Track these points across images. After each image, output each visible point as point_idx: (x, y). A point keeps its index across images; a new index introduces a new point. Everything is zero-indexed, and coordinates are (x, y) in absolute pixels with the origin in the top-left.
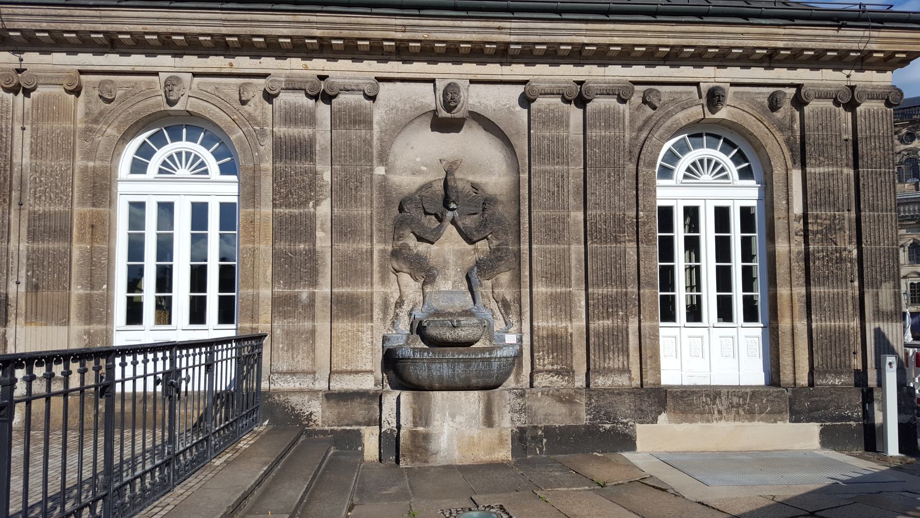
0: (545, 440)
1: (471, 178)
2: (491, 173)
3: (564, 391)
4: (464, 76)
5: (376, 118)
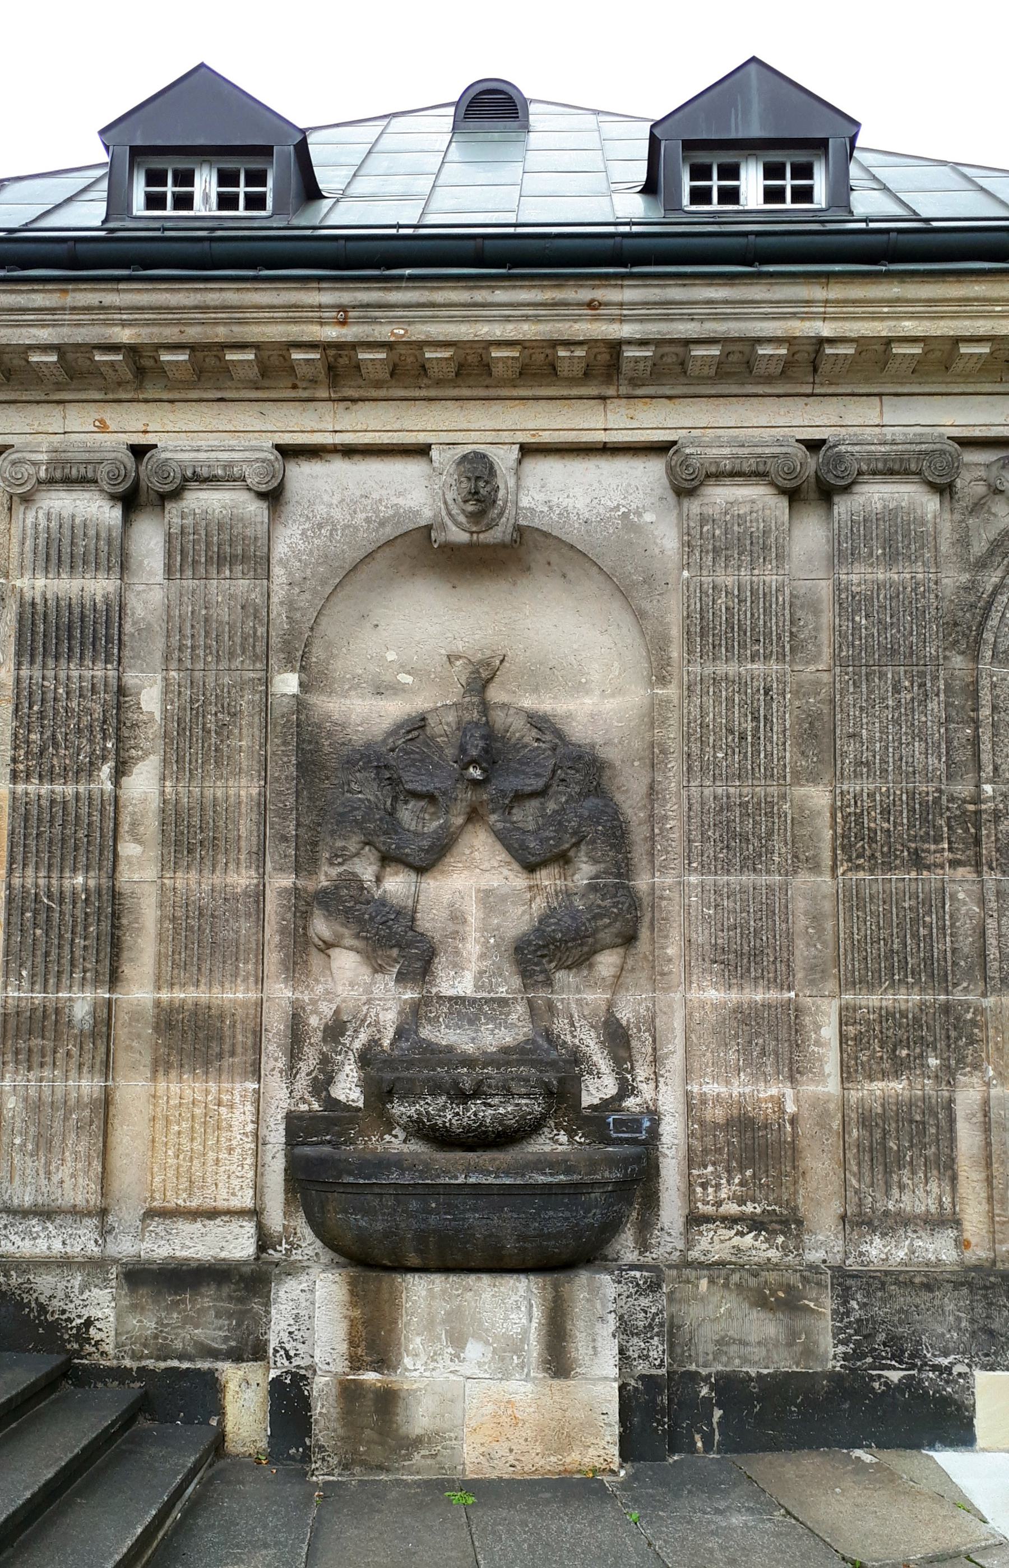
0: (718, 1413)
1: (528, 702)
2: (580, 688)
3: (772, 1277)
4: (506, 437)
5: (281, 549)
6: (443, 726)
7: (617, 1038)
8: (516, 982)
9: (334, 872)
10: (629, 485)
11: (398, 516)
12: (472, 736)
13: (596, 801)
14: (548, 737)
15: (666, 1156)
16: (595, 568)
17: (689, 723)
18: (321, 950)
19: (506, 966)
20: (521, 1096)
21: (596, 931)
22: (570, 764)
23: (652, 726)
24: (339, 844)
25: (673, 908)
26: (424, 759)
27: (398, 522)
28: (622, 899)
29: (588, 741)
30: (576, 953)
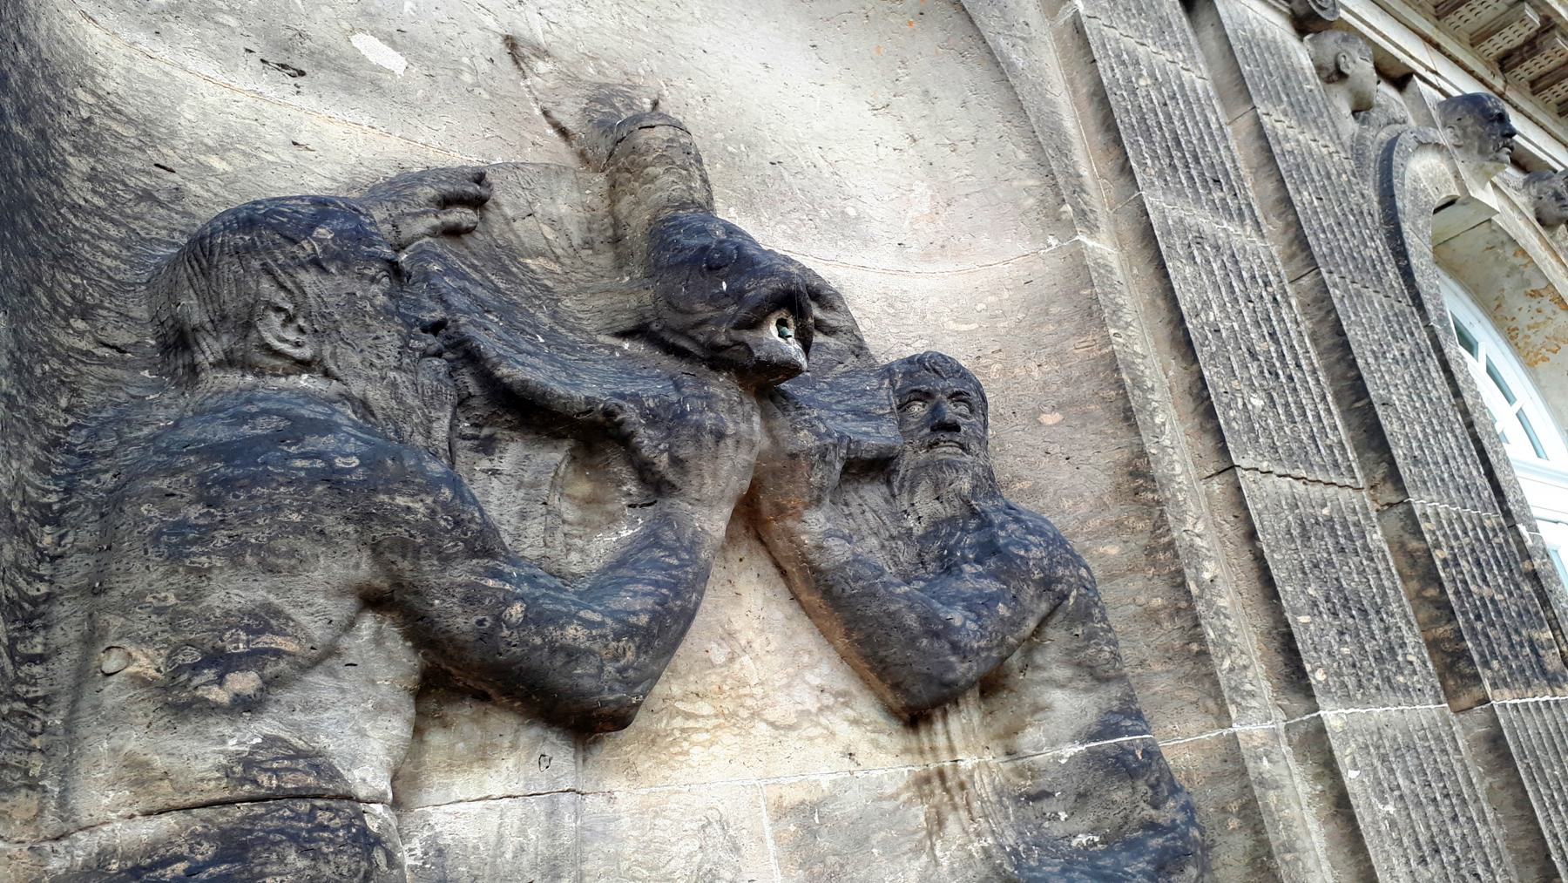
9: (202, 755)
24: (233, 593)
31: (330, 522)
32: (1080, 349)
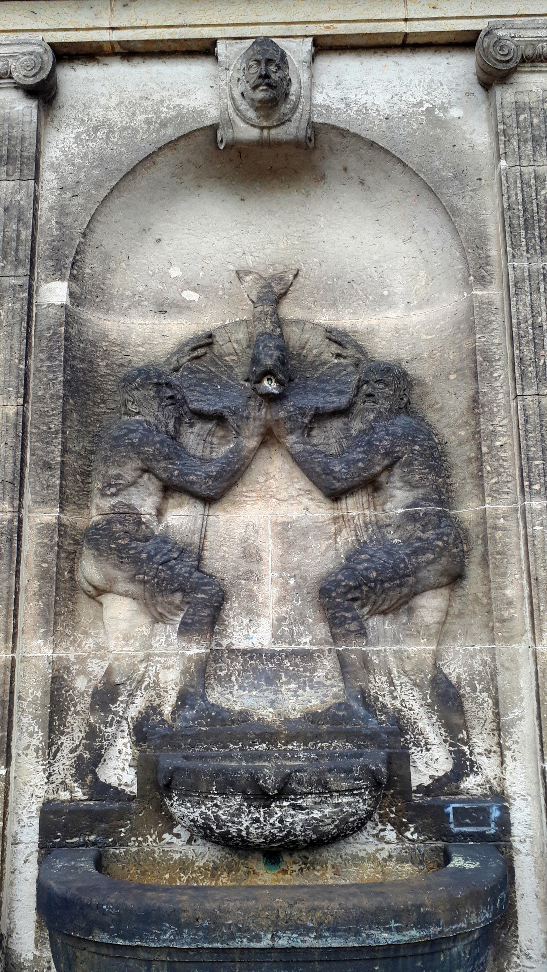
1: (326, 318)
2: (383, 301)
4: (298, 30)
5: (52, 153)
6: (234, 345)
7: (447, 699)
8: (322, 630)
9: (106, 504)
10: (432, 81)
11: (181, 115)
12: (265, 346)
13: (408, 419)
14: (350, 352)
15: (519, 852)
16: (399, 167)
17: (519, 324)
18: (91, 597)
19: (309, 612)
20: (341, 793)
21: (418, 568)
22: (377, 377)
23: (472, 329)
24: (113, 471)
25: (511, 539)
26: (212, 379)
27: (181, 123)
28: (447, 530)
29: (393, 357)
30: (394, 595)
31: (131, 455)
32: (466, 344)
